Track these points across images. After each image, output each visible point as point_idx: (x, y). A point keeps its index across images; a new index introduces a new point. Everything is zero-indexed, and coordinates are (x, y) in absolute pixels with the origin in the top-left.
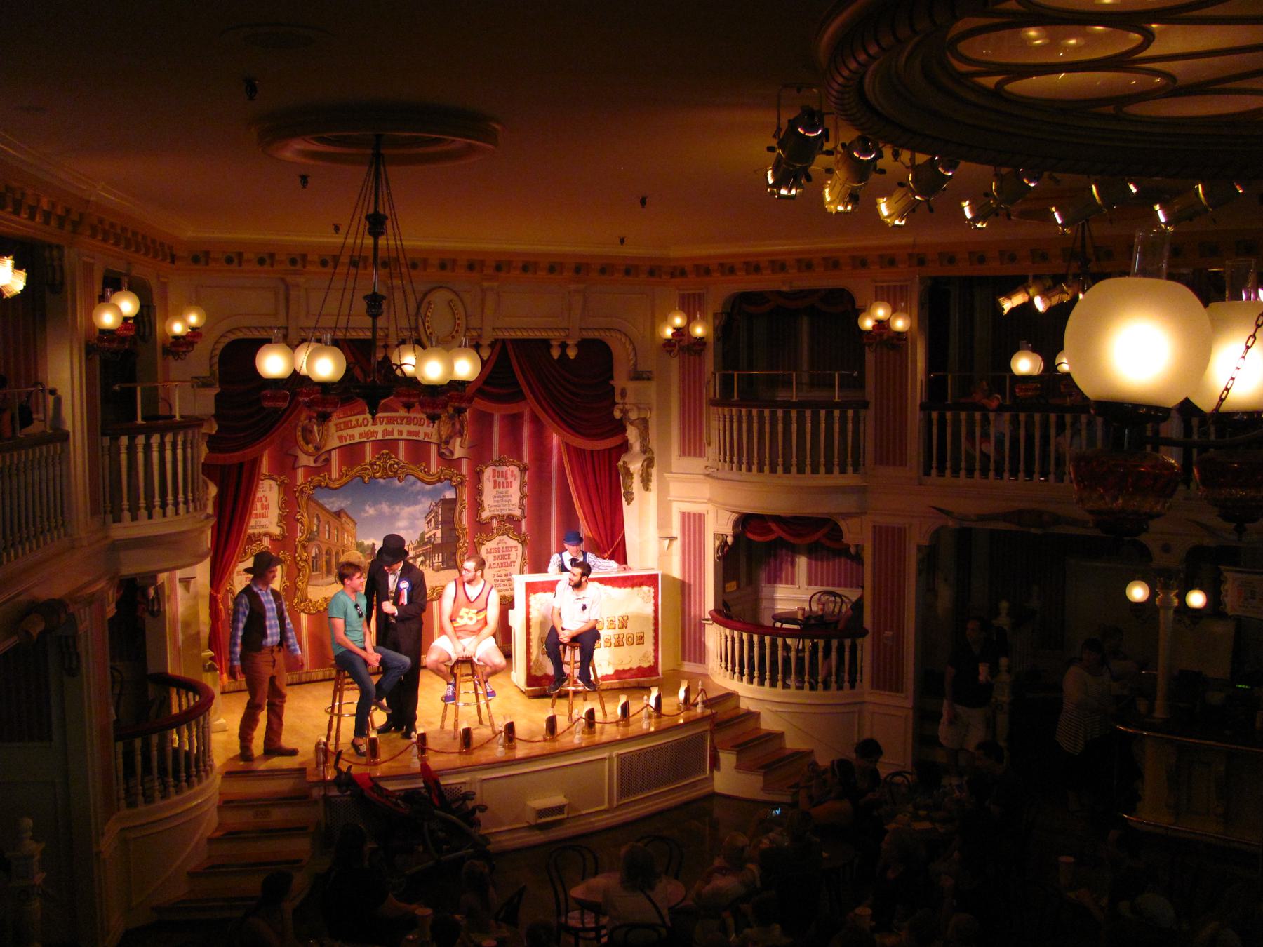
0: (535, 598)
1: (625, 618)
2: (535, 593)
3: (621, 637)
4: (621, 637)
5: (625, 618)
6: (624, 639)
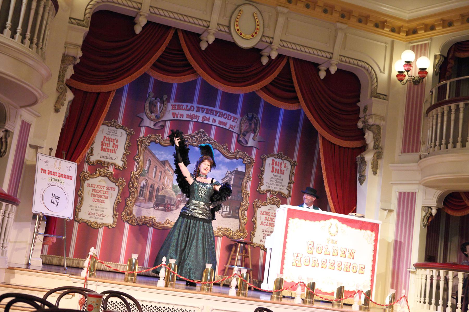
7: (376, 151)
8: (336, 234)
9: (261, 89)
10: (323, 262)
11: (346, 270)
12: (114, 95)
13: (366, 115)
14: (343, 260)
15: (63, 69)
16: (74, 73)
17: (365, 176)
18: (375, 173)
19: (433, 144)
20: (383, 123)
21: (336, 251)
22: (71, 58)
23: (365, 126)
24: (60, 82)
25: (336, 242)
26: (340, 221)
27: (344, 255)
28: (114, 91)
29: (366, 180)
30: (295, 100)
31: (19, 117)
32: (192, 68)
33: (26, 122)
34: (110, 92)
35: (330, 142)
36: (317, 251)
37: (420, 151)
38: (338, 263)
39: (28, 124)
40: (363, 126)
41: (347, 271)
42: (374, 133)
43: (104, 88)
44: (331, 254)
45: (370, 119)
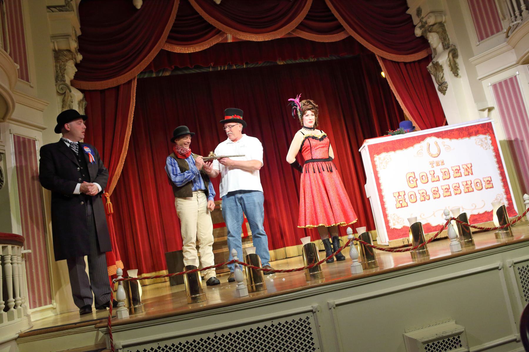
0: (380, 158)
1: (469, 166)
2: (378, 154)
3: (469, 183)
4: (469, 183)
5: (469, 166)
6: (473, 185)
7: (448, 50)
8: (439, 153)
9: (297, 28)
10: (434, 191)
11: (468, 191)
12: (136, 84)
13: (423, 18)
14: (459, 180)
15: (60, 67)
16: (77, 70)
17: (446, 83)
18: (456, 74)
19: (513, 17)
20: (445, 18)
21: (446, 173)
22: (65, 52)
23: (425, 32)
24: (59, 82)
25: (443, 162)
26: (438, 137)
27: (459, 174)
28: (134, 79)
29: (448, 87)
30: (339, 28)
31: (8, 132)
32: (215, 28)
33: (24, 139)
34: (130, 82)
35: (392, 61)
36: (422, 181)
37: (502, 29)
38: (454, 186)
39: (29, 140)
40: (422, 33)
41: (470, 191)
42: (438, 33)
43: (121, 80)
44: (441, 179)
45: (429, 18)
